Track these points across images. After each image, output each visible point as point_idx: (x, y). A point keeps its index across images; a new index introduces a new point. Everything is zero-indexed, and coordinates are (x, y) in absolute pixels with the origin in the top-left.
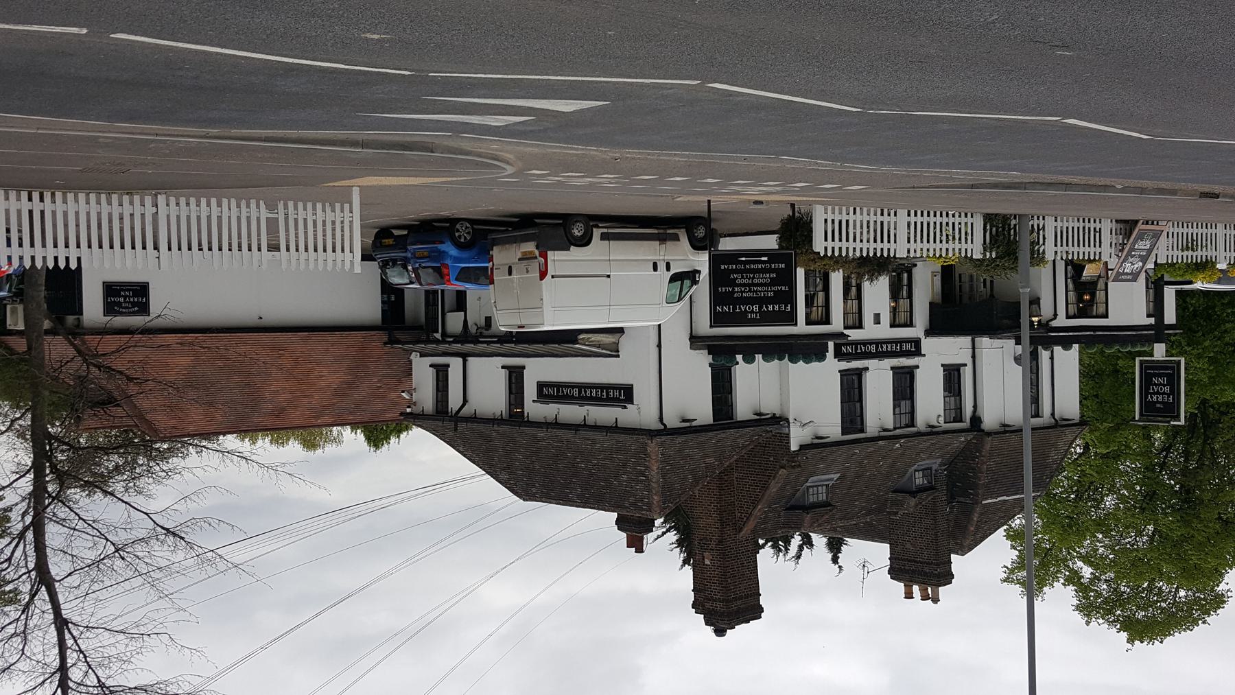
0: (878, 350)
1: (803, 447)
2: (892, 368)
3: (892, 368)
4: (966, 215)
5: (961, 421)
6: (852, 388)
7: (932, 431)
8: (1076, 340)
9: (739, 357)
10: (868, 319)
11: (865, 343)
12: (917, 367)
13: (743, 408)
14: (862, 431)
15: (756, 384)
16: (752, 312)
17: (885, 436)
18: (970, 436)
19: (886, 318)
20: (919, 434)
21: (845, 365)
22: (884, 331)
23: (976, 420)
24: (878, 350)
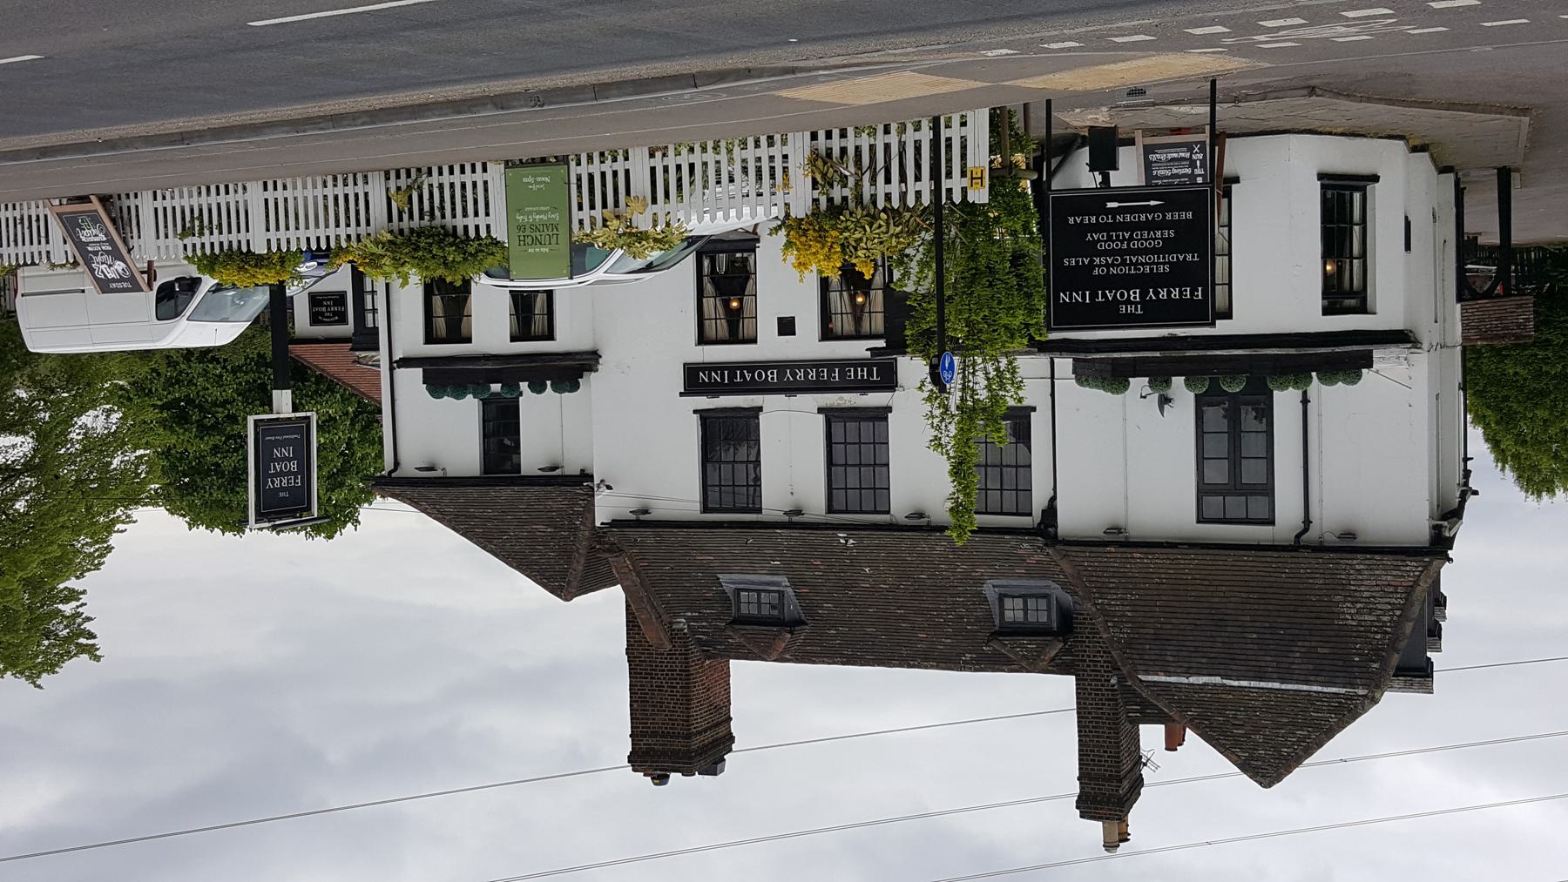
0: (789, 378)
1: (616, 523)
2: (820, 410)
3: (820, 410)
4: (590, 158)
5: (1030, 514)
6: (728, 442)
7: (920, 526)
8: (1136, 369)
9: (524, 386)
10: (766, 326)
11: (752, 366)
12: (889, 409)
13: (531, 458)
14: (759, 511)
15: (547, 426)
16: (1128, 302)
17: (795, 522)
18: (1040, 541)
19: (808, 323)
20: (892, 527)
21: (704, 402)
22: (807, 344)
23: (1050, 511)
24: (789, 378)
